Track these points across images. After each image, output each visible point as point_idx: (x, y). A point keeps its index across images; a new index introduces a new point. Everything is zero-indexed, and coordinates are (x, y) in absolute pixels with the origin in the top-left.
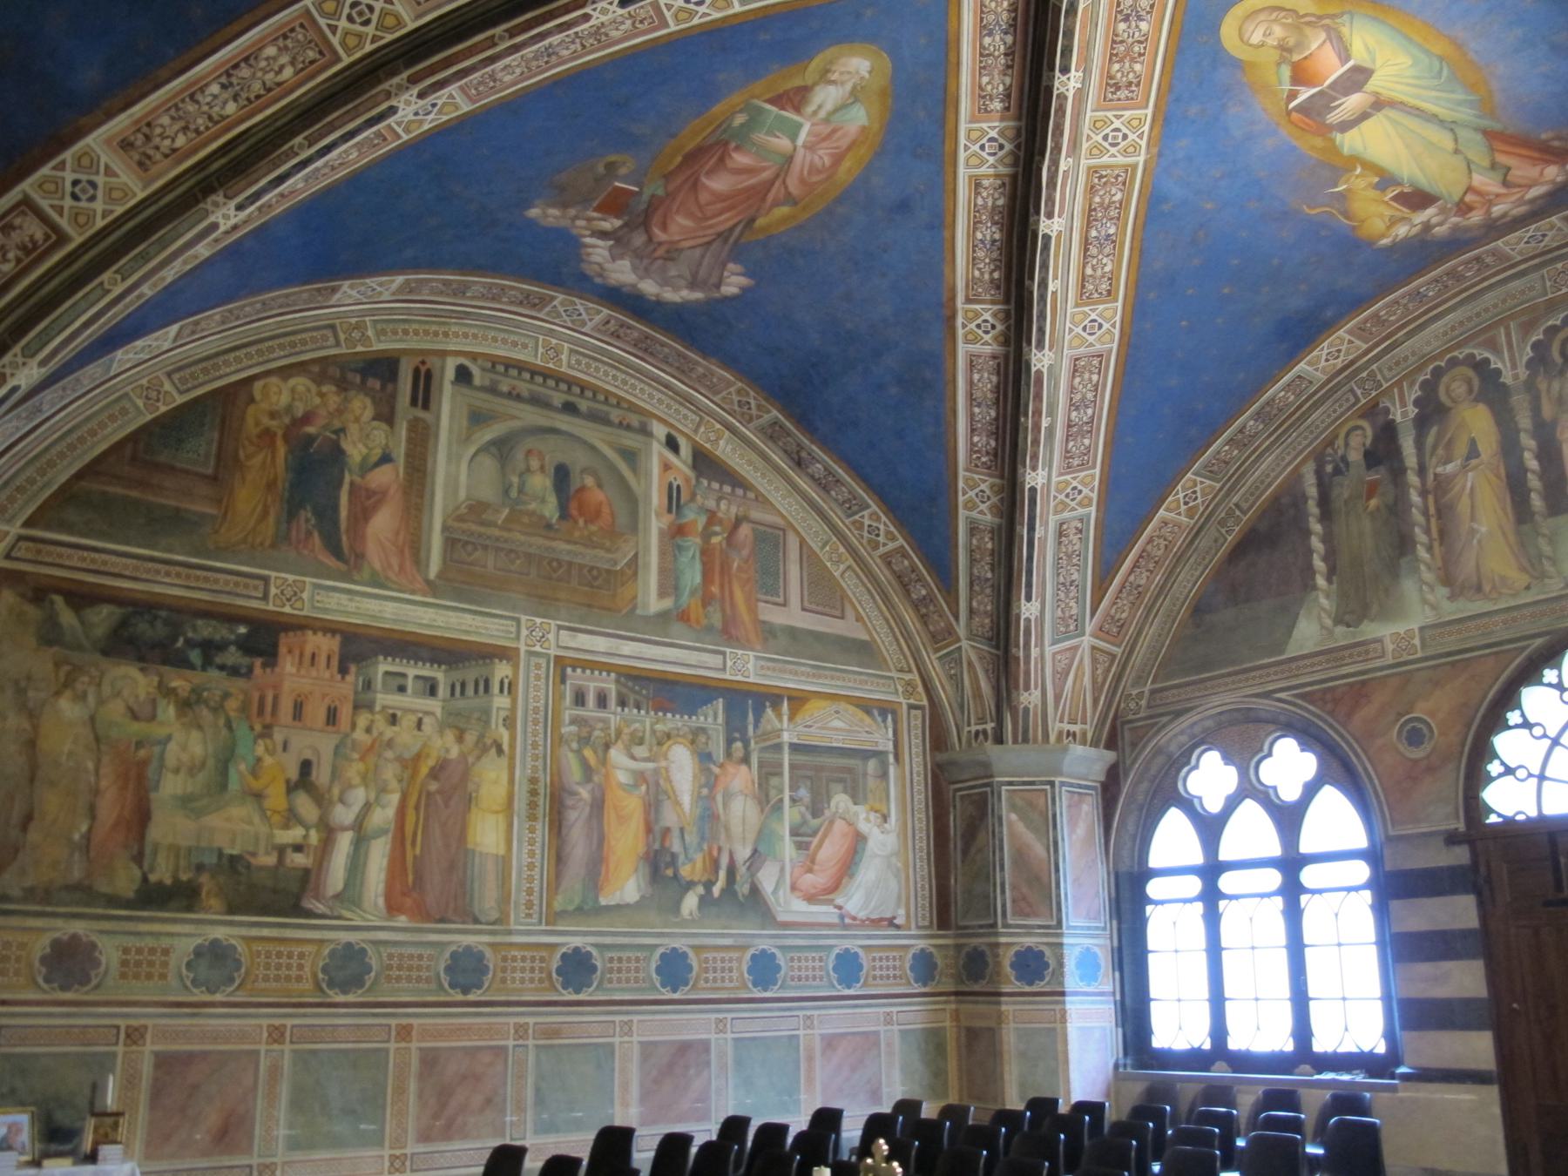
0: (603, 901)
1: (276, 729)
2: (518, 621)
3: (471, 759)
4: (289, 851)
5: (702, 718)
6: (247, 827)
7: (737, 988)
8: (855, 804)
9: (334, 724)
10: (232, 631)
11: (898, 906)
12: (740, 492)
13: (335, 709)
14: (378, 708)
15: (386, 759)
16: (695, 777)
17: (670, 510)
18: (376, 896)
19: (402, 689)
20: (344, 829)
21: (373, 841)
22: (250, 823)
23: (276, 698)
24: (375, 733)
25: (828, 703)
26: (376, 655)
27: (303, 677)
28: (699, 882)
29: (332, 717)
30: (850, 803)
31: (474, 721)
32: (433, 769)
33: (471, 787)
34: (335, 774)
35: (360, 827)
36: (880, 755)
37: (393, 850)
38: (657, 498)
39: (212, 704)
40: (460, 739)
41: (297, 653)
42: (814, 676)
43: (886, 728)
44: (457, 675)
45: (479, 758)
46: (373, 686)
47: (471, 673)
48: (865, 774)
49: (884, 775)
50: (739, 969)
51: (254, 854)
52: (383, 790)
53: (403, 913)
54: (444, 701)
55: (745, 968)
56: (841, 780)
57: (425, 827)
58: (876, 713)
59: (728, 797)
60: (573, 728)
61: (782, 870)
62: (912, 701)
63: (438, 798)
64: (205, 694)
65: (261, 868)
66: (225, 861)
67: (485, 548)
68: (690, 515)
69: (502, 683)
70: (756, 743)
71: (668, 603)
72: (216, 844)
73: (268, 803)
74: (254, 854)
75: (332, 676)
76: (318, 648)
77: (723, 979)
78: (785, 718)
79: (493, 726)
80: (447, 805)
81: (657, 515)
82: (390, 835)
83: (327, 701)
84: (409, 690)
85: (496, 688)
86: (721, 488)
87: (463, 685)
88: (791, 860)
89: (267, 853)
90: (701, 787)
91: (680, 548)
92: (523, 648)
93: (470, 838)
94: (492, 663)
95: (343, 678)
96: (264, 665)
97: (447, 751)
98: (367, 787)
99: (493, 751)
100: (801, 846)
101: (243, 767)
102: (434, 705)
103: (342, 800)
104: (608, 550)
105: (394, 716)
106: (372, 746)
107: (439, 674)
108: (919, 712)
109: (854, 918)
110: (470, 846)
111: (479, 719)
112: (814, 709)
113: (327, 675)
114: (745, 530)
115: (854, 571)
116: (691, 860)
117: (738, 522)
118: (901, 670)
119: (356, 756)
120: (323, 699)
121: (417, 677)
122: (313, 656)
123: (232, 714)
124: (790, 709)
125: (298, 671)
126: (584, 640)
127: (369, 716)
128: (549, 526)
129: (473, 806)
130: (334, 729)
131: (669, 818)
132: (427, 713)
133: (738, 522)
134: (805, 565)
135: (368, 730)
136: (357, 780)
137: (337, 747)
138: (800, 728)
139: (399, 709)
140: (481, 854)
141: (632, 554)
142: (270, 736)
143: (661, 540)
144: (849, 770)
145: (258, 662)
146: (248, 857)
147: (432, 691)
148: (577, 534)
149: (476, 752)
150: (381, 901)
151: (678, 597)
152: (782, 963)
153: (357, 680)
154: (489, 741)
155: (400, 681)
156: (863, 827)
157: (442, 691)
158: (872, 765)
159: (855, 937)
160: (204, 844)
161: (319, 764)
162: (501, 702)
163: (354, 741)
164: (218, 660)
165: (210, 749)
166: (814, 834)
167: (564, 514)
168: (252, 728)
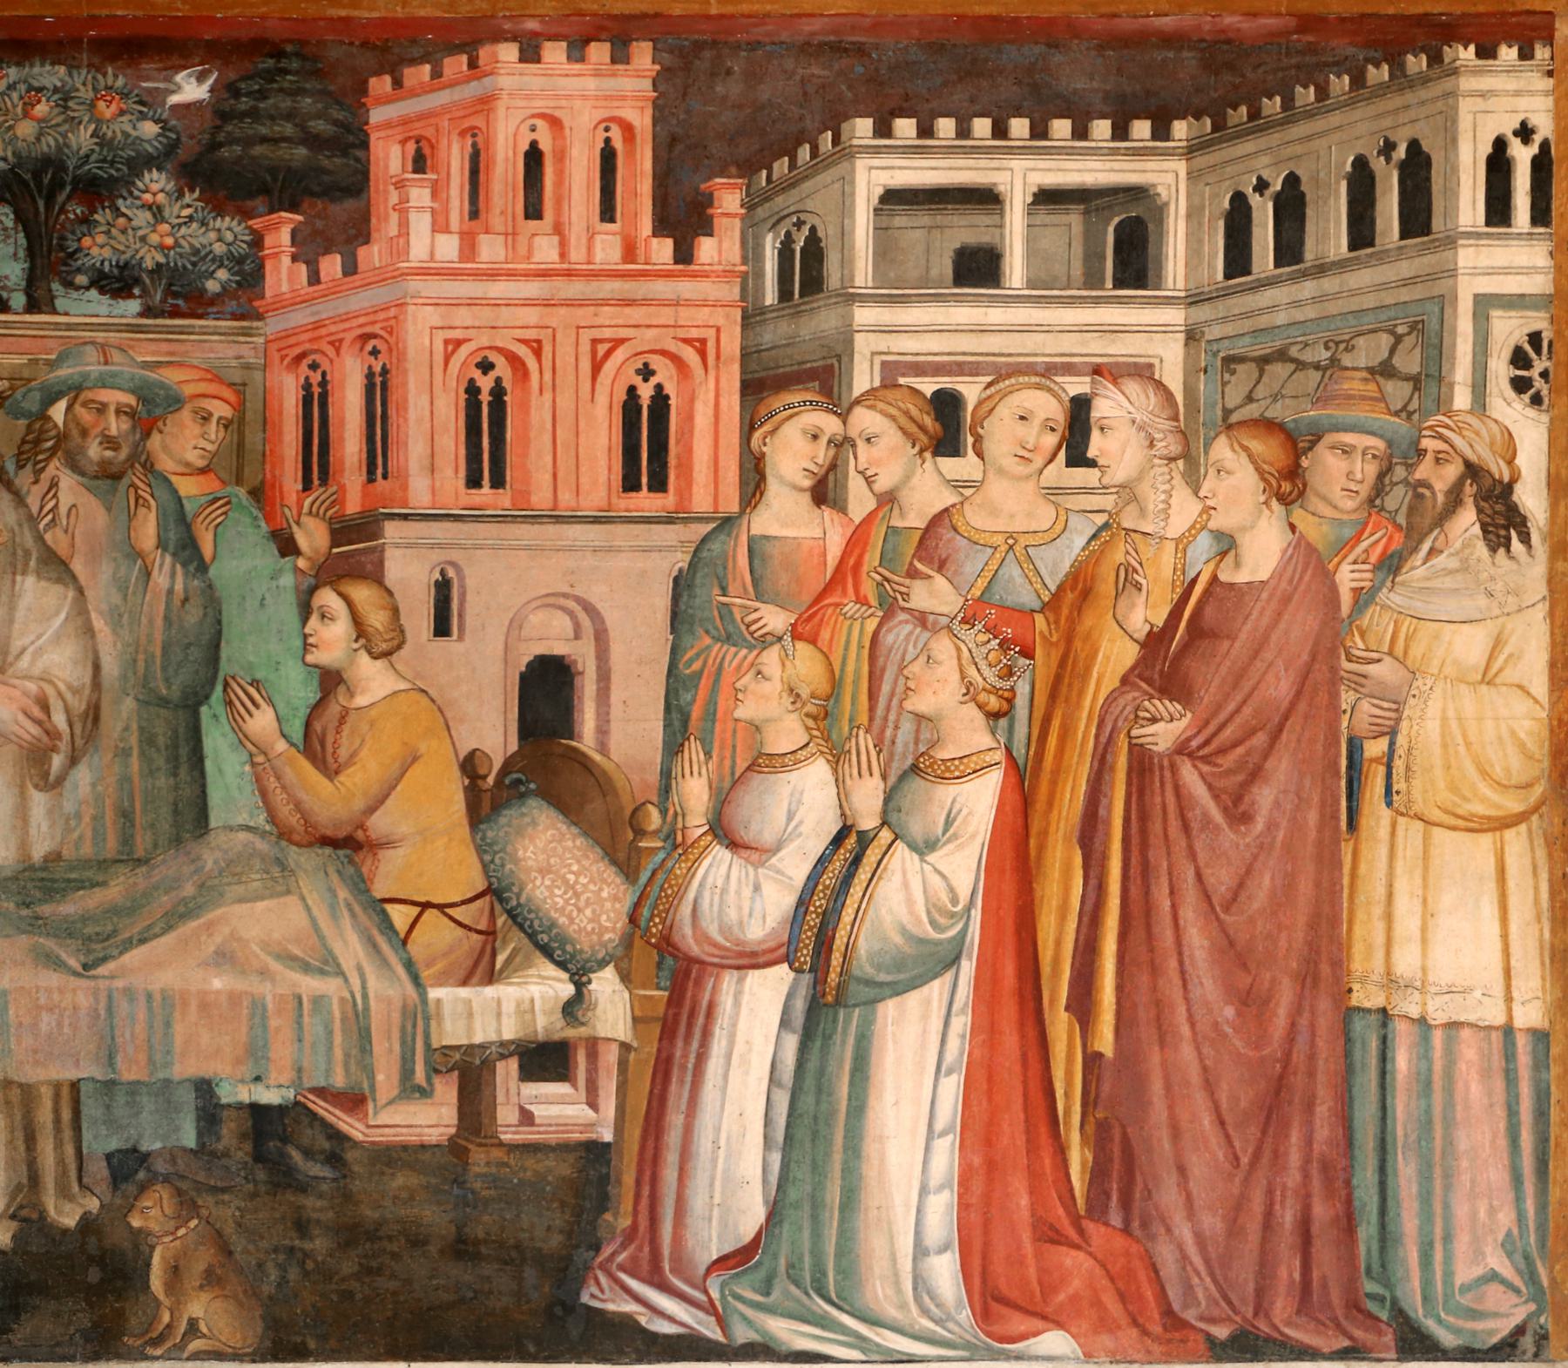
1: (392, 530)
3: (1347, 577)
4: (507, 1070)
6: (310, 985)
9: (659, 484)
10: (147, 104)
13: (661, 399)
14: (863, 378)
15: (922, 618)
18: (920, 1251)
20: (752, 960)
21: (889, 1009)
22: (328, 965)
23: (379, 389)
24: (860, 502)
26: (835, 121)
27: (492, 275)
31: (1354, 384)
32: (1154, 642)
33: (1357, 711)
35: (824, 943)
37: (985, 1029)
39: (94, 451)
41: (455, 158)
45: (1391, 565)
46: (833, 277)
51: (354, 1101)
53: (1060, 1325)
54: (1194, 299)
57: (1136, 918)
63: (1189, 775)
64: (58, 412)
65: (392, 1156)
66: (228, 1135)
69: (1498, 164)
72: (186, 1068)
73: (388, 876)
74: (354, 1101)
75: (629, 252)
76: (555, 123)
79: (1462, 399)
80: (1238, 812)
82: (968, 968)
83: (619, 372)
84: (1015, 270)
89: (412, 1090)
93: (1365, 961)
95: (684, 255)
96: (308, 249)
97: (1227, 545)
98: (837, 758)
99: (1467, 520)
101: (262, 722)
103: (722, 831)
105: (946, 405)
106: (846, 572)
110: (1366, 996)
111: (1386, 370)
113: (607, 249)
119: (775, 619)
120: (596, 368)
121: (1048, 198)
122: (534, 157)
123: (188, 487)
125: (469, 247)
127: (830, 424)
129: (1376, 815)
130: (665, 502)
135: (825, 492)
136: (787, 733)
137: (681, 585)
139: (959, 369)
140: (1422, 1022)
142: (376, 576)
145: (281, 232)
146: (321, 1107)
149: (1375, 542)
150: (945, 1271)
153: (751, 253)
154: (1443, 478)
155: (965, 229)
160: (129, 1073)
161: (604, 677)
163: (752, 541)
164: (99, 249)
165: (111, 667)
168: (287, 546)
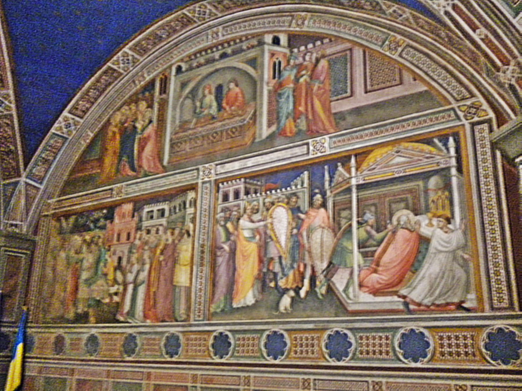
0: (235, 306)
2: (198, 169)
5: (294, 187)
7: (317, 358)
8: (416, 215)
11: (467, 291)
12: (318, 43)
14: (143, 228)
16: (289, 223)
17: (274, 77)
19: (152, 217)
24: (142, 240)
25: (390, 148)
28: (291, 288)
29: (128, 238)
30: (411, 215)
34: (129, 261)
36: (444, 172)
38: (267, 73)
40: (173, 234)
42: (377, 133)
43: (448, 149)
44: (173, 204)
47: (177, 202)
48: (426, 191)
49: (448, 186)
50: (319, 346)
52: (144, 264)
55: (323, 344)
56: (402, 200)
58: (436, 141)
59: (310, 231)
60: (222, 214)
61: (351, 273)
62: (476, 119)
67: (185, 141)
68: (286, 74)
70: (331, 192)
71: (274, 128)
77: (307, 352)
78: (353, 170)
81: (268, 83)
85: (188, 205)
86: (306, 47)
87: (175, 208)
88: (359, 266)
90: (293, 229)
91: (280, 95)
92: (200, 181)
94: (187, 193)
100: (365, 255)
102: (164, 221)
104: (241, 116)
107: (166, 206)
108: (485, 126)
109: (419, 305)
112: (377, 155)
114: (323, 63)
115: (412, 47)
116: (285, 275)
117: (318, 60)
118: (464, 99)
124: (356, 161)
126: (229, 167)
128: (213, 118)
131: (273, 252)
132: (161, 225)
133: (318, 60)
134: (368, 62)
138: (365, 172)
141: (253, 111)
143: (269, 97)
144: (410, 191)
147: (163, 215)
148: (225, 114)
151: (279, 123)
152: (353, 341)
155: (150, 214)
156: (425, 231)
157: (167, 213)
158: (433, 181)
159: (421, 320)
162: (190, 210)
166: (379, 245)
167: (220, 108)
